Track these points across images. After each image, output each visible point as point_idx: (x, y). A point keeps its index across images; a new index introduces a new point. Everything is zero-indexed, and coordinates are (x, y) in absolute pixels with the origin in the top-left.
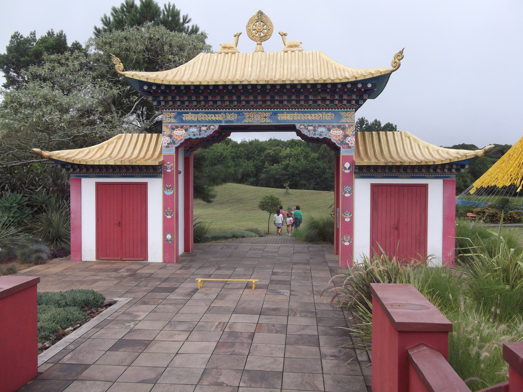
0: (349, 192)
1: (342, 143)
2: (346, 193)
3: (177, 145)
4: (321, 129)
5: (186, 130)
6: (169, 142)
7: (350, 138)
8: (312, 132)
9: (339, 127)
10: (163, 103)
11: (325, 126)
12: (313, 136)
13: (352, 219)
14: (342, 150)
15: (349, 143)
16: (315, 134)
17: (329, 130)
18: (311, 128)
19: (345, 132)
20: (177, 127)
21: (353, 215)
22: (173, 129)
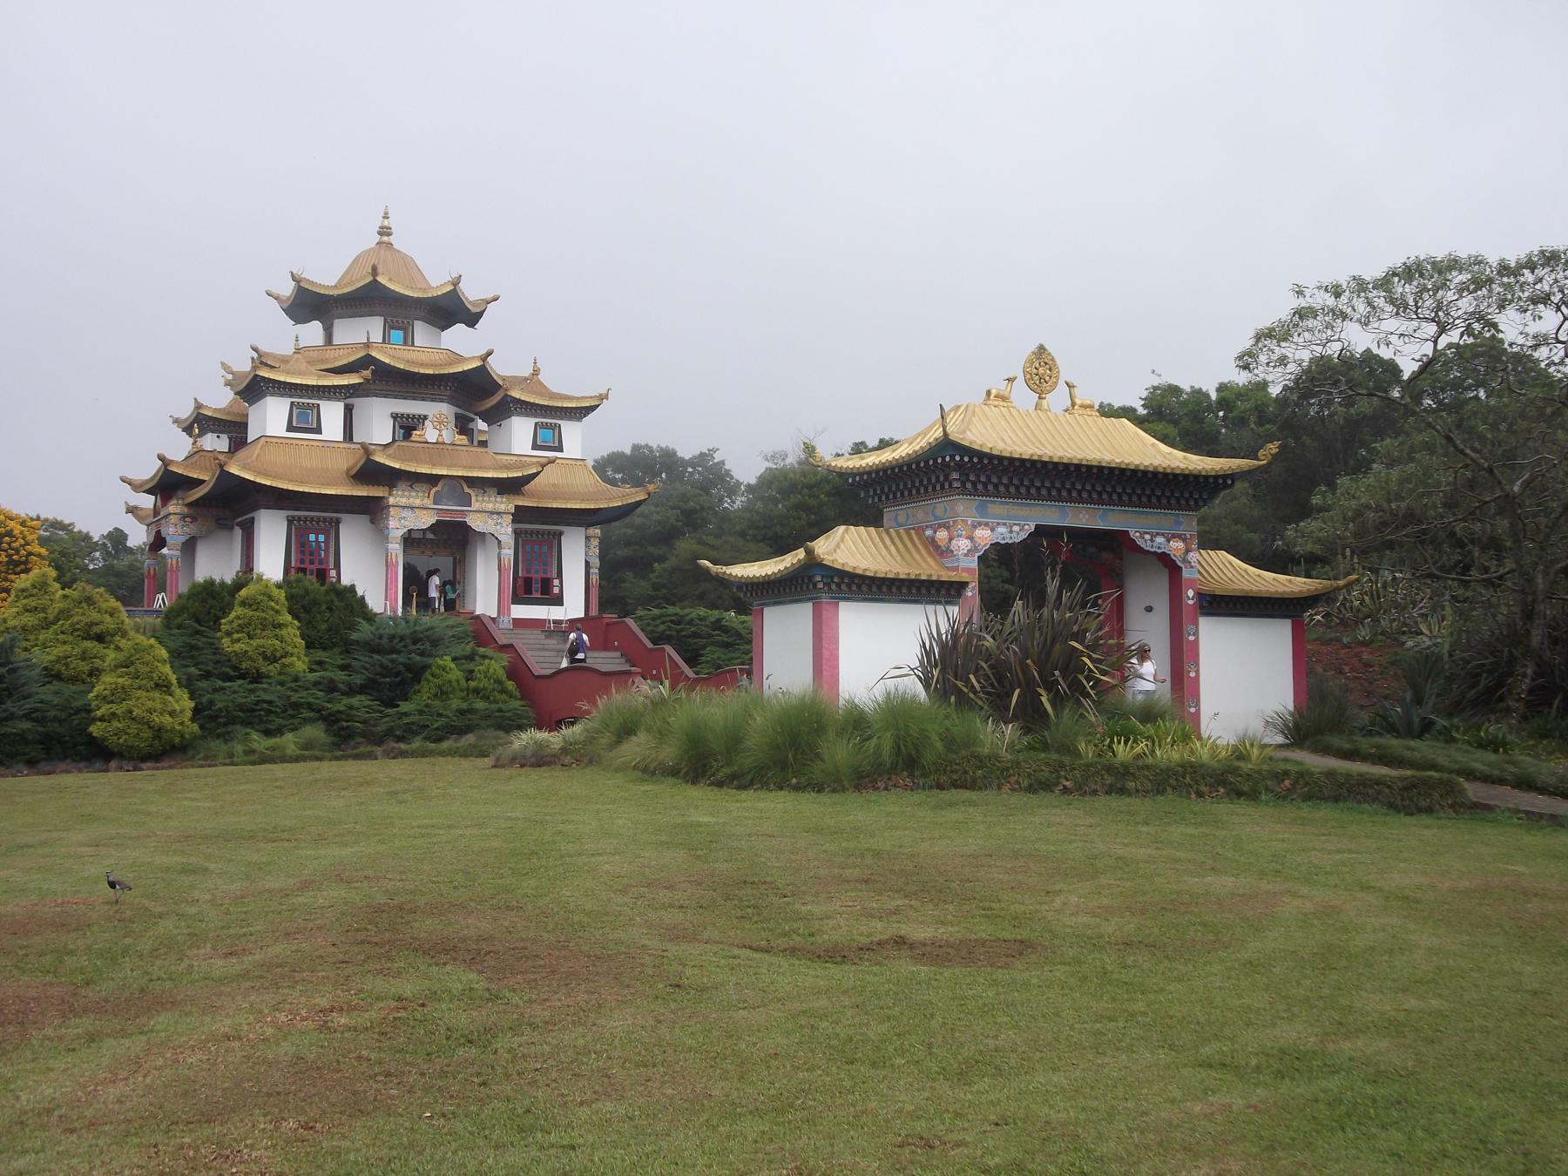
1: (1184, 560)
4: (1160, 540)
5: (993, 530)
13: (1197, 672)
18: (1147, 537)
20: (980, 524)
22: (974, 527)
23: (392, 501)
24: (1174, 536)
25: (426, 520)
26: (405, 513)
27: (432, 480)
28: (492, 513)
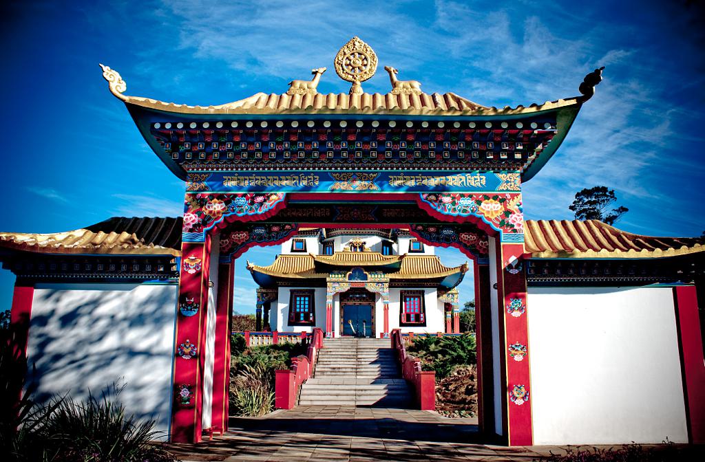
0: (520, 309)
1: (503, 224)
2: (513, 310)
3: (208, 228)
4: (466, 202)
6: (196, 222)
7: (514, 216)
8: (449, 206)
9: (495, 198)
10: (189, 156)
11: (471, 196)
12: (451, 213)
13: (526, 357)
14: (502, 235)
15: (515, 224)
16: (454, 210)
17: (479, 202)
19: (505, 206)
21: (527, 349)
23: (328, 279)
24: (487, 197)
25: (345, 287)
26: (337, 285)
27: (347, 268)
28: (379, 283)
